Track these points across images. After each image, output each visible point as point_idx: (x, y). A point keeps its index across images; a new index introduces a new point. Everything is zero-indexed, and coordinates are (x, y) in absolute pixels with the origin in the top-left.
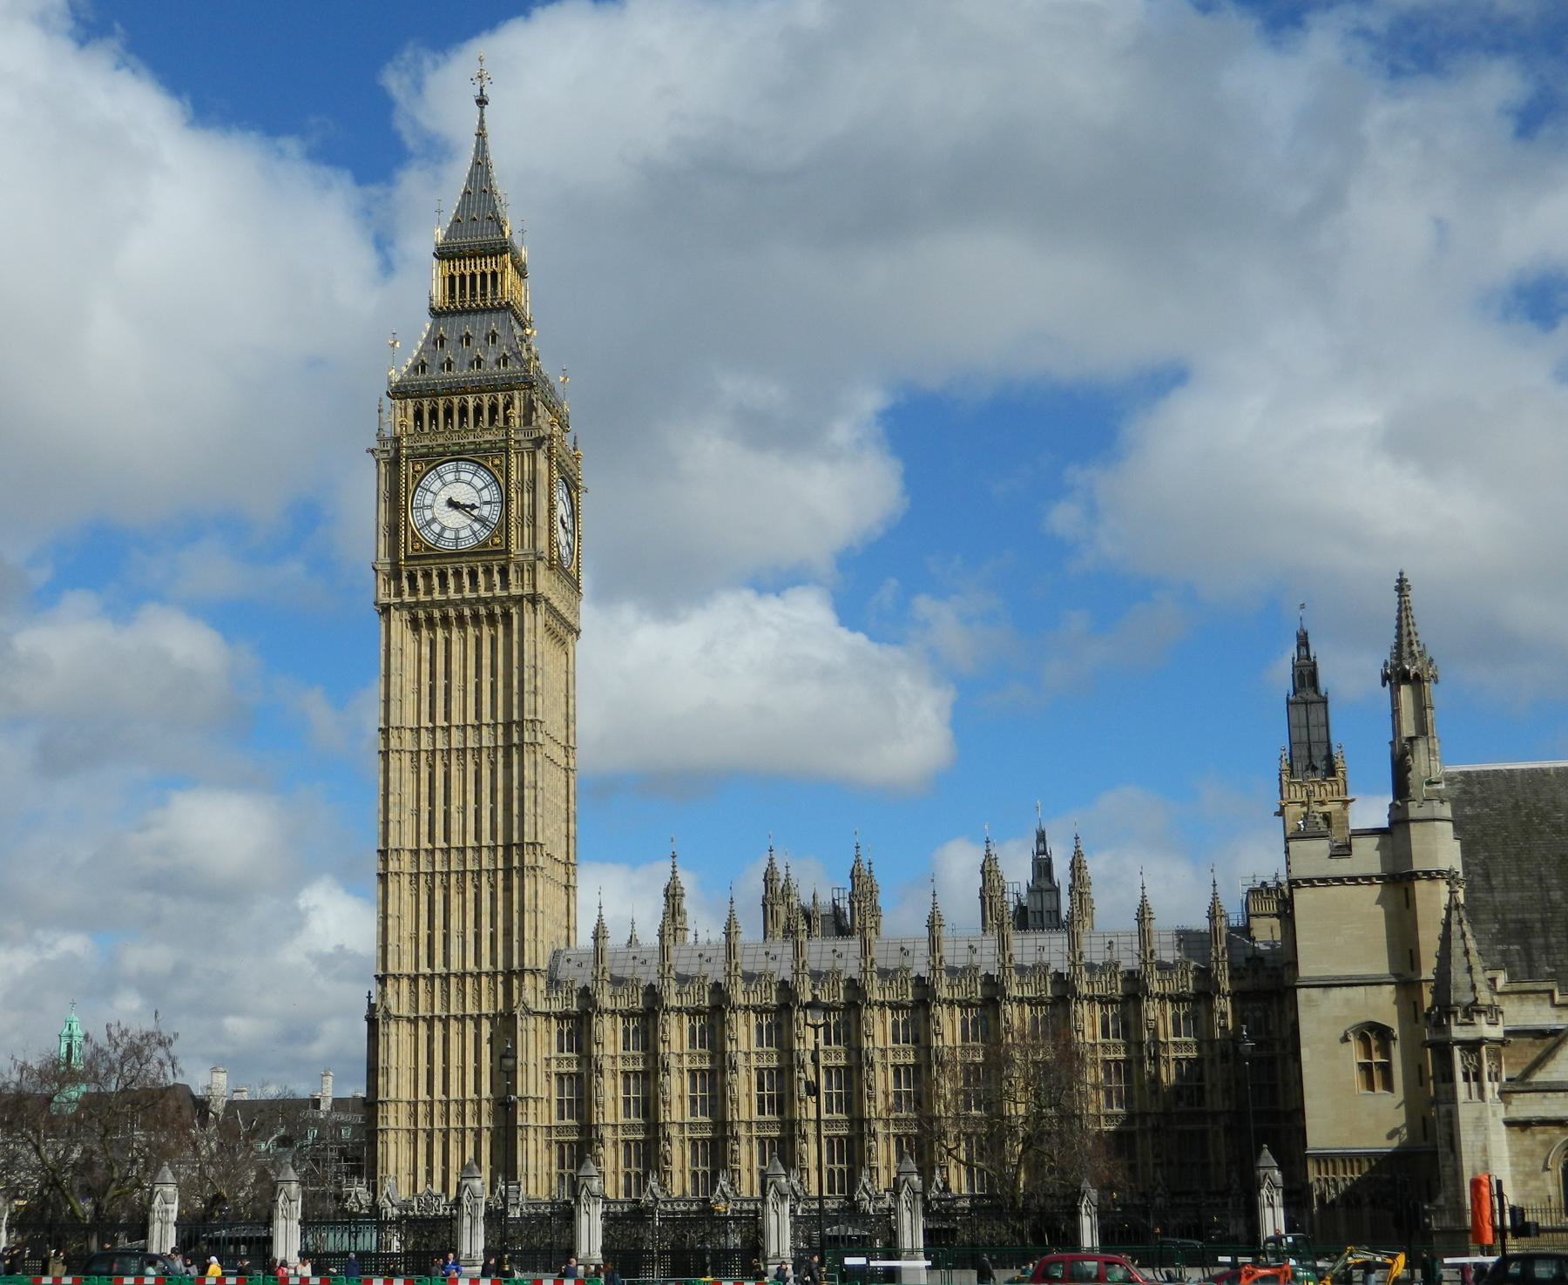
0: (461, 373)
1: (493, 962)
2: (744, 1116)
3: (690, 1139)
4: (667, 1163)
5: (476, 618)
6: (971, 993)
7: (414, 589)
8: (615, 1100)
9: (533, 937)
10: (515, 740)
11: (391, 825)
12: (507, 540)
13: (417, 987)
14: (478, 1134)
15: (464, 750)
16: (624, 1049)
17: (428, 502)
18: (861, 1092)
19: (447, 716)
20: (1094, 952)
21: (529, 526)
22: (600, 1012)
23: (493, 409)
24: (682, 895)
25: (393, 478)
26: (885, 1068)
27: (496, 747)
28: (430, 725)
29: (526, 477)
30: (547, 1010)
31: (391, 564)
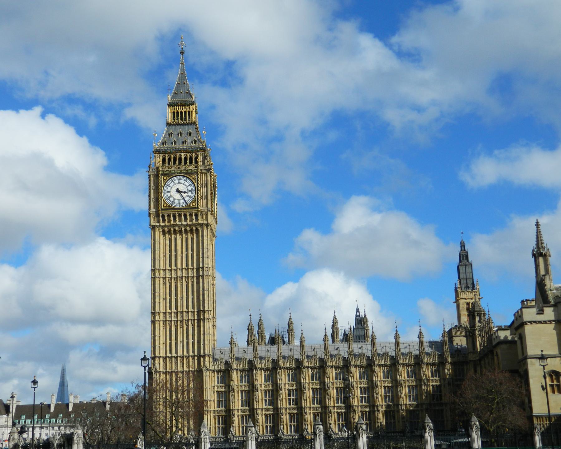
0: (179, 146)
1: (194, 352)
4: (257, 423)
5: (186, 231)
6: (362, 363)
7: (164, 221)
8: (238, 400)
9: (208, 343)
10: (201, 274)
12: (198, 204)
13: (166, 361)
15: (182, 277)
16: (241, 383)
17: (169, 190)
18: (325, 397)
19: (176, 265)
21: (205, 199)
22: (256, 369)
23: (191, 158)
26: (333, 389)
27: (193, 277)
28: (170, 268)
29: (204, 182)
30: (213, 369)
31: (156, 211)
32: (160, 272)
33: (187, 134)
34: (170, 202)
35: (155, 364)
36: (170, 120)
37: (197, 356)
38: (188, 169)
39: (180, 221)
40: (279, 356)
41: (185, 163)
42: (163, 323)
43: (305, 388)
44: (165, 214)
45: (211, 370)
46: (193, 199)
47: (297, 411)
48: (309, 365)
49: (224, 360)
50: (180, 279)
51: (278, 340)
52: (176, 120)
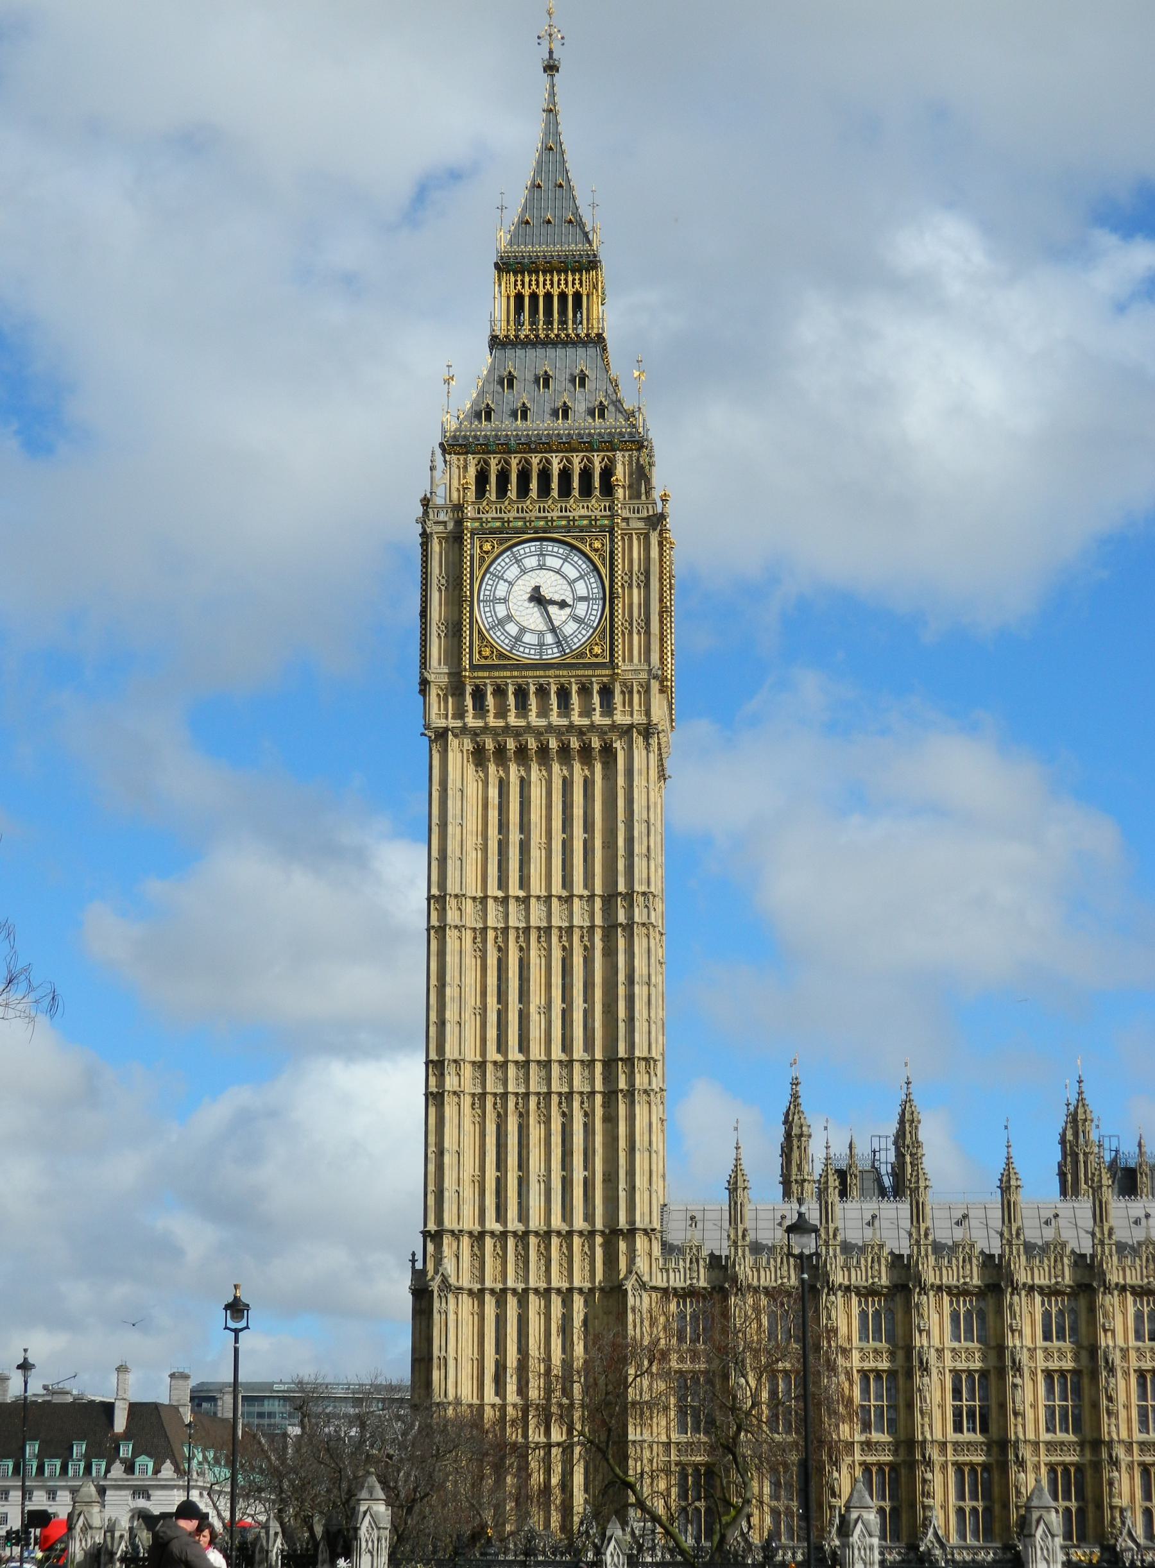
0: (541, 424)
1: (589, 1217)
2: (938, 1436)
3: (955, 1464)
4: (834, 1495)
5: (565, 752)
7: (480, 708)
9: (646, 1185)
10: (621, 918)
11: (448, 1027)
12: (612, 650)
13: (482, 1248)
14: (567, 1448)
15: (548, 929)
18: (1095, 1406)
19: (524, 882)
20: (943, 1232)
21: (639, 633)
23: (586, 474)
24: (810, 1136)
25: (450, 559)
26: (1126, 1374)
27: (592, 928)
28: (500, 894)
29: (636, 568)
30: (665, 1285)
31: (449, 674)
32: (463, 909)
33: (570, 381)
34: (507, 641)
35: (441, 1259)
36: (504, 324)
37: (603, 1232)
38: (576, 514)
39: (544, 712)
40: (918, 1242)
41: (565, 491)
42: (473, 1104)
43: (1018, 1369)
44: (485, 685)
45: (654, 1288)
46: (595, 629)
47: (988, 1453)
48: (1033, 1279)
49: (705, 1253)
50: (539, 937)
51: (917, 1182)
52: (527, 326)
